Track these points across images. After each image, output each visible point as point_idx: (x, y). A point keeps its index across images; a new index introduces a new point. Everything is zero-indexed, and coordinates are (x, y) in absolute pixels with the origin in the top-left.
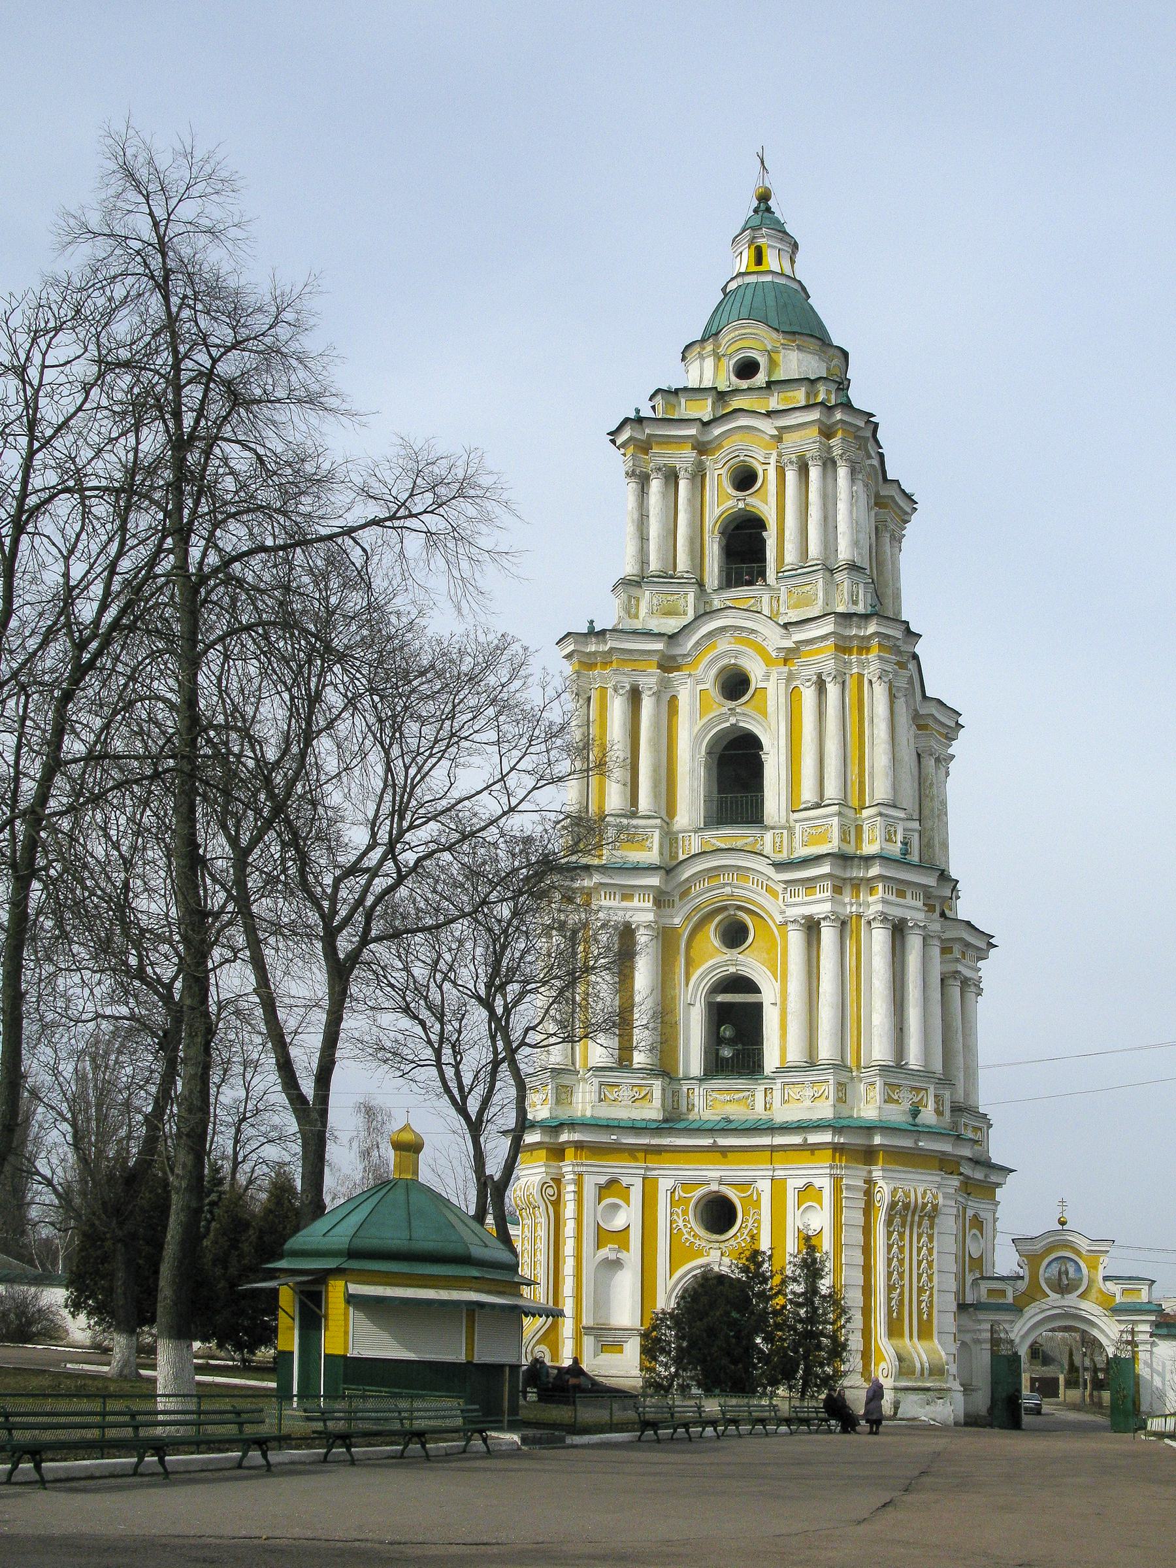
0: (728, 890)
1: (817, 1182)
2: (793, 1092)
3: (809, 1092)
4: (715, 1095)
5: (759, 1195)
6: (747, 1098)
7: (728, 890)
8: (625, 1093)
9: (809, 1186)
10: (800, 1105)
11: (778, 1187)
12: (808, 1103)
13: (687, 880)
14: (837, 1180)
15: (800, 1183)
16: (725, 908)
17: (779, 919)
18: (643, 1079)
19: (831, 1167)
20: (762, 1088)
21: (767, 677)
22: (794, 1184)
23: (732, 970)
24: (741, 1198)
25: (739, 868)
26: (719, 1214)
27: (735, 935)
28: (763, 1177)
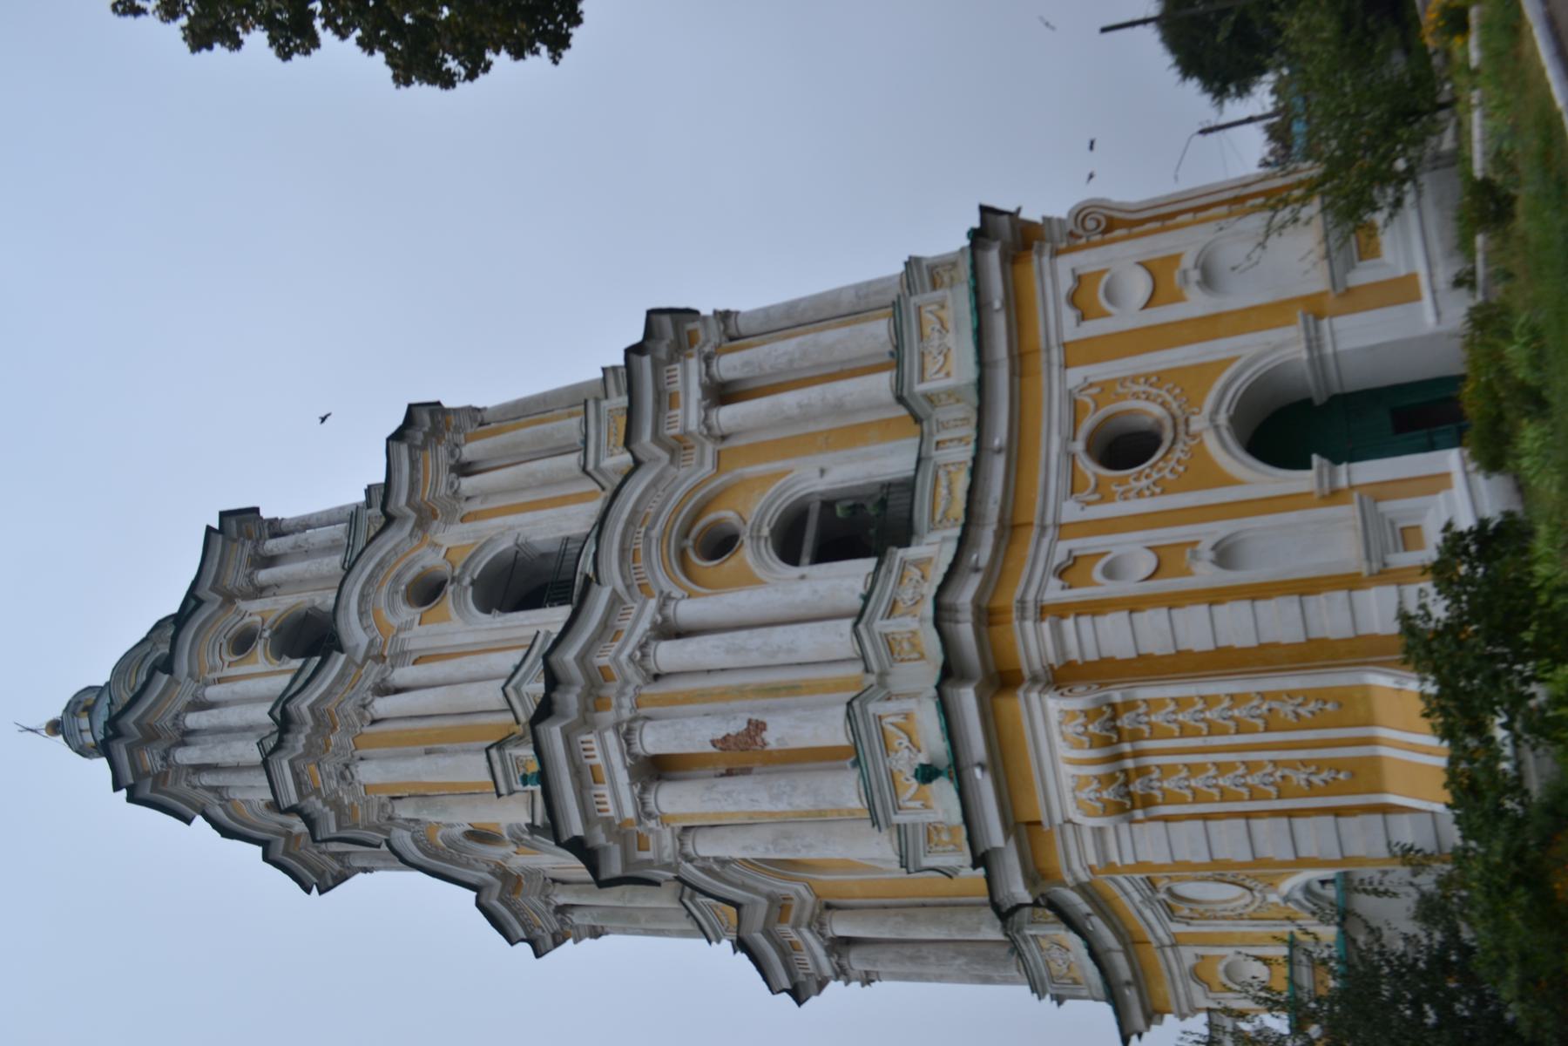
0: (655, 533)
1: (1066, 283)
2: (931, 368)
3: (934, 341)
4: (938, 517)
5: (1091, 385)
6: (949, 473)
7: (655, 533)
8: (907, 594)
9: (1072, 300)
10: (953, 356)
11: (1075, 354)
12: (950, 340)
13: (628, 587)
14: (1056, 253)
15: (1069, 315)
16: (682, 555)
17: (708, 467)
18: (890, 571)
19: (1040, 255)
20: (934, 453)
21: (436, 546)
22: (1071, 328)
23: (766, 531)
24: (1097, 408)
25: (630, 522)
26: (1125, 447)
27: (721, 544)
28: (1063, 380)
